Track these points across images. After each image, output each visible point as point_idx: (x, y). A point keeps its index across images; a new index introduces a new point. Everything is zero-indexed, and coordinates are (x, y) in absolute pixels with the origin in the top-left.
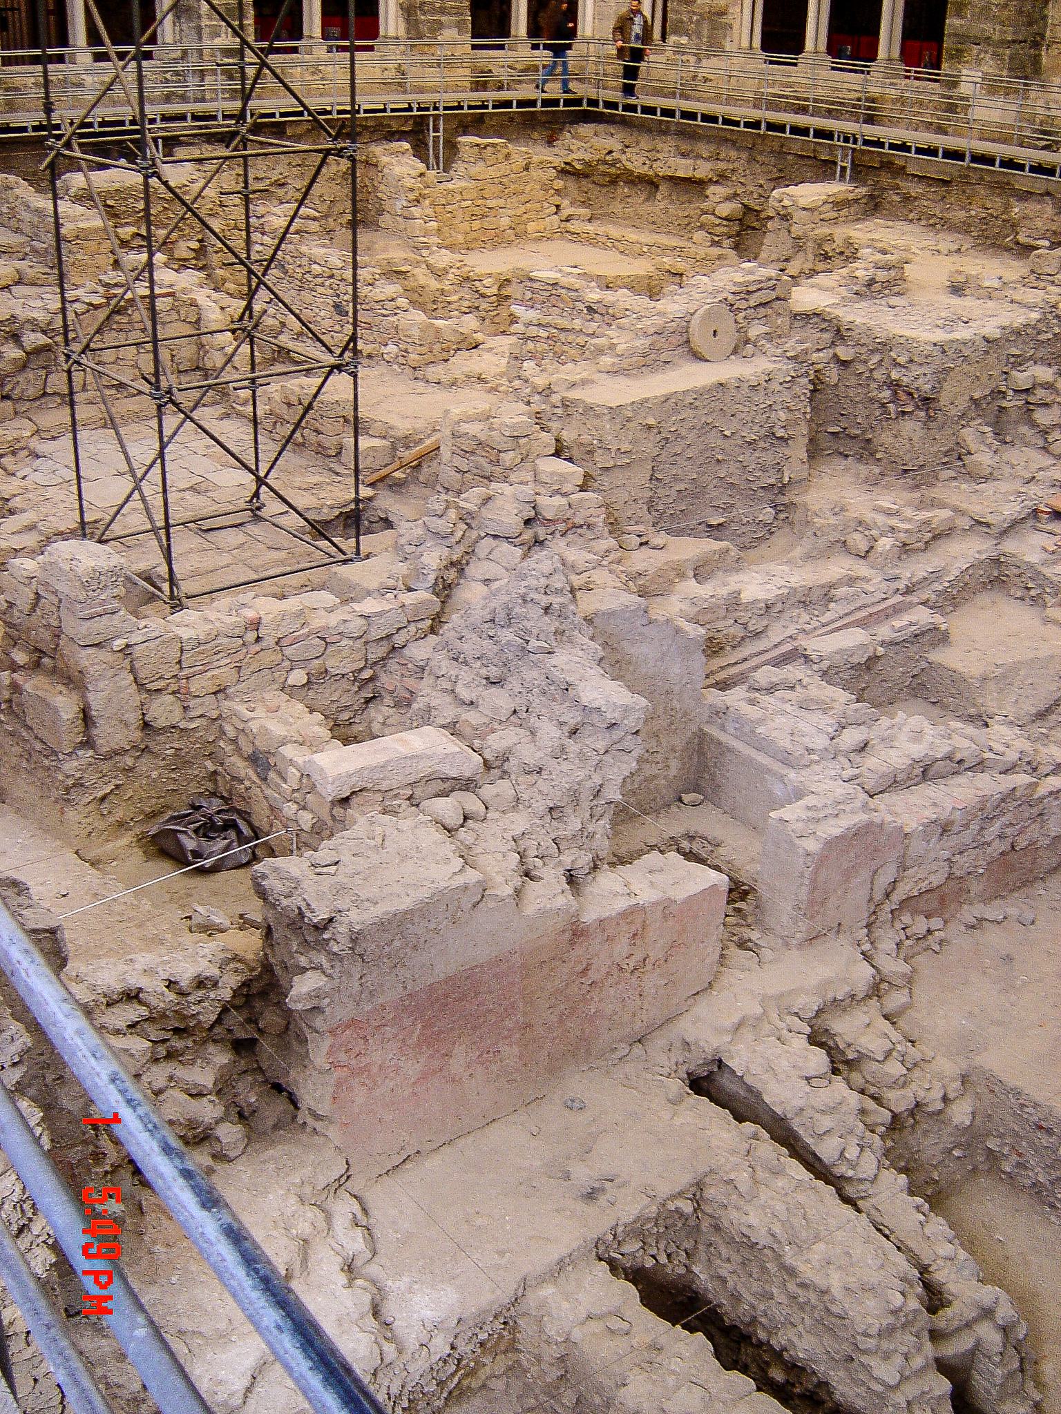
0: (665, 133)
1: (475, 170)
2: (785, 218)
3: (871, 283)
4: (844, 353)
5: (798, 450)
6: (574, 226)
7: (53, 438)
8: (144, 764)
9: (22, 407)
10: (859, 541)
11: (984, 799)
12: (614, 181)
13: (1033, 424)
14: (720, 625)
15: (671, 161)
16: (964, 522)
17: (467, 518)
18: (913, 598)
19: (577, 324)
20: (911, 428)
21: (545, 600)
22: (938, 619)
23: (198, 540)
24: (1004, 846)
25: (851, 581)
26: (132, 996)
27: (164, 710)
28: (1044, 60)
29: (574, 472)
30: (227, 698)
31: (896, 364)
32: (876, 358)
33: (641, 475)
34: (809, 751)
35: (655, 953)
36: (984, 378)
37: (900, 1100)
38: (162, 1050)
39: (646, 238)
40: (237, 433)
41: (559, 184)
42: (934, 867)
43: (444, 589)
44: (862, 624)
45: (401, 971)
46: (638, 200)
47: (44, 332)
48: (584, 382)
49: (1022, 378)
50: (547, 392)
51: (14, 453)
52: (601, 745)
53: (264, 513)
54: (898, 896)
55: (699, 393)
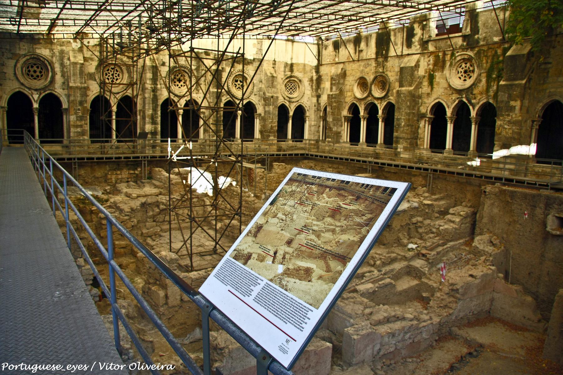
0: (325, 162)
1: (278, 170)
7: (166, 232)
9: (158, 224)
11: (404, 328)
13: (417, 232)
16: (399, 257)
22: (392, 281)
24: (411, 341)
25: (370, 272)
28: (419, 143)
34: (356, 314)
35: (312, 364)
36: (404, 220)
40: (212, 233)
44: (372, 283)
45: (242, 363)
47: (165, 205)
49: (414, 220)
51: (155, 235)
54: (381, 353)
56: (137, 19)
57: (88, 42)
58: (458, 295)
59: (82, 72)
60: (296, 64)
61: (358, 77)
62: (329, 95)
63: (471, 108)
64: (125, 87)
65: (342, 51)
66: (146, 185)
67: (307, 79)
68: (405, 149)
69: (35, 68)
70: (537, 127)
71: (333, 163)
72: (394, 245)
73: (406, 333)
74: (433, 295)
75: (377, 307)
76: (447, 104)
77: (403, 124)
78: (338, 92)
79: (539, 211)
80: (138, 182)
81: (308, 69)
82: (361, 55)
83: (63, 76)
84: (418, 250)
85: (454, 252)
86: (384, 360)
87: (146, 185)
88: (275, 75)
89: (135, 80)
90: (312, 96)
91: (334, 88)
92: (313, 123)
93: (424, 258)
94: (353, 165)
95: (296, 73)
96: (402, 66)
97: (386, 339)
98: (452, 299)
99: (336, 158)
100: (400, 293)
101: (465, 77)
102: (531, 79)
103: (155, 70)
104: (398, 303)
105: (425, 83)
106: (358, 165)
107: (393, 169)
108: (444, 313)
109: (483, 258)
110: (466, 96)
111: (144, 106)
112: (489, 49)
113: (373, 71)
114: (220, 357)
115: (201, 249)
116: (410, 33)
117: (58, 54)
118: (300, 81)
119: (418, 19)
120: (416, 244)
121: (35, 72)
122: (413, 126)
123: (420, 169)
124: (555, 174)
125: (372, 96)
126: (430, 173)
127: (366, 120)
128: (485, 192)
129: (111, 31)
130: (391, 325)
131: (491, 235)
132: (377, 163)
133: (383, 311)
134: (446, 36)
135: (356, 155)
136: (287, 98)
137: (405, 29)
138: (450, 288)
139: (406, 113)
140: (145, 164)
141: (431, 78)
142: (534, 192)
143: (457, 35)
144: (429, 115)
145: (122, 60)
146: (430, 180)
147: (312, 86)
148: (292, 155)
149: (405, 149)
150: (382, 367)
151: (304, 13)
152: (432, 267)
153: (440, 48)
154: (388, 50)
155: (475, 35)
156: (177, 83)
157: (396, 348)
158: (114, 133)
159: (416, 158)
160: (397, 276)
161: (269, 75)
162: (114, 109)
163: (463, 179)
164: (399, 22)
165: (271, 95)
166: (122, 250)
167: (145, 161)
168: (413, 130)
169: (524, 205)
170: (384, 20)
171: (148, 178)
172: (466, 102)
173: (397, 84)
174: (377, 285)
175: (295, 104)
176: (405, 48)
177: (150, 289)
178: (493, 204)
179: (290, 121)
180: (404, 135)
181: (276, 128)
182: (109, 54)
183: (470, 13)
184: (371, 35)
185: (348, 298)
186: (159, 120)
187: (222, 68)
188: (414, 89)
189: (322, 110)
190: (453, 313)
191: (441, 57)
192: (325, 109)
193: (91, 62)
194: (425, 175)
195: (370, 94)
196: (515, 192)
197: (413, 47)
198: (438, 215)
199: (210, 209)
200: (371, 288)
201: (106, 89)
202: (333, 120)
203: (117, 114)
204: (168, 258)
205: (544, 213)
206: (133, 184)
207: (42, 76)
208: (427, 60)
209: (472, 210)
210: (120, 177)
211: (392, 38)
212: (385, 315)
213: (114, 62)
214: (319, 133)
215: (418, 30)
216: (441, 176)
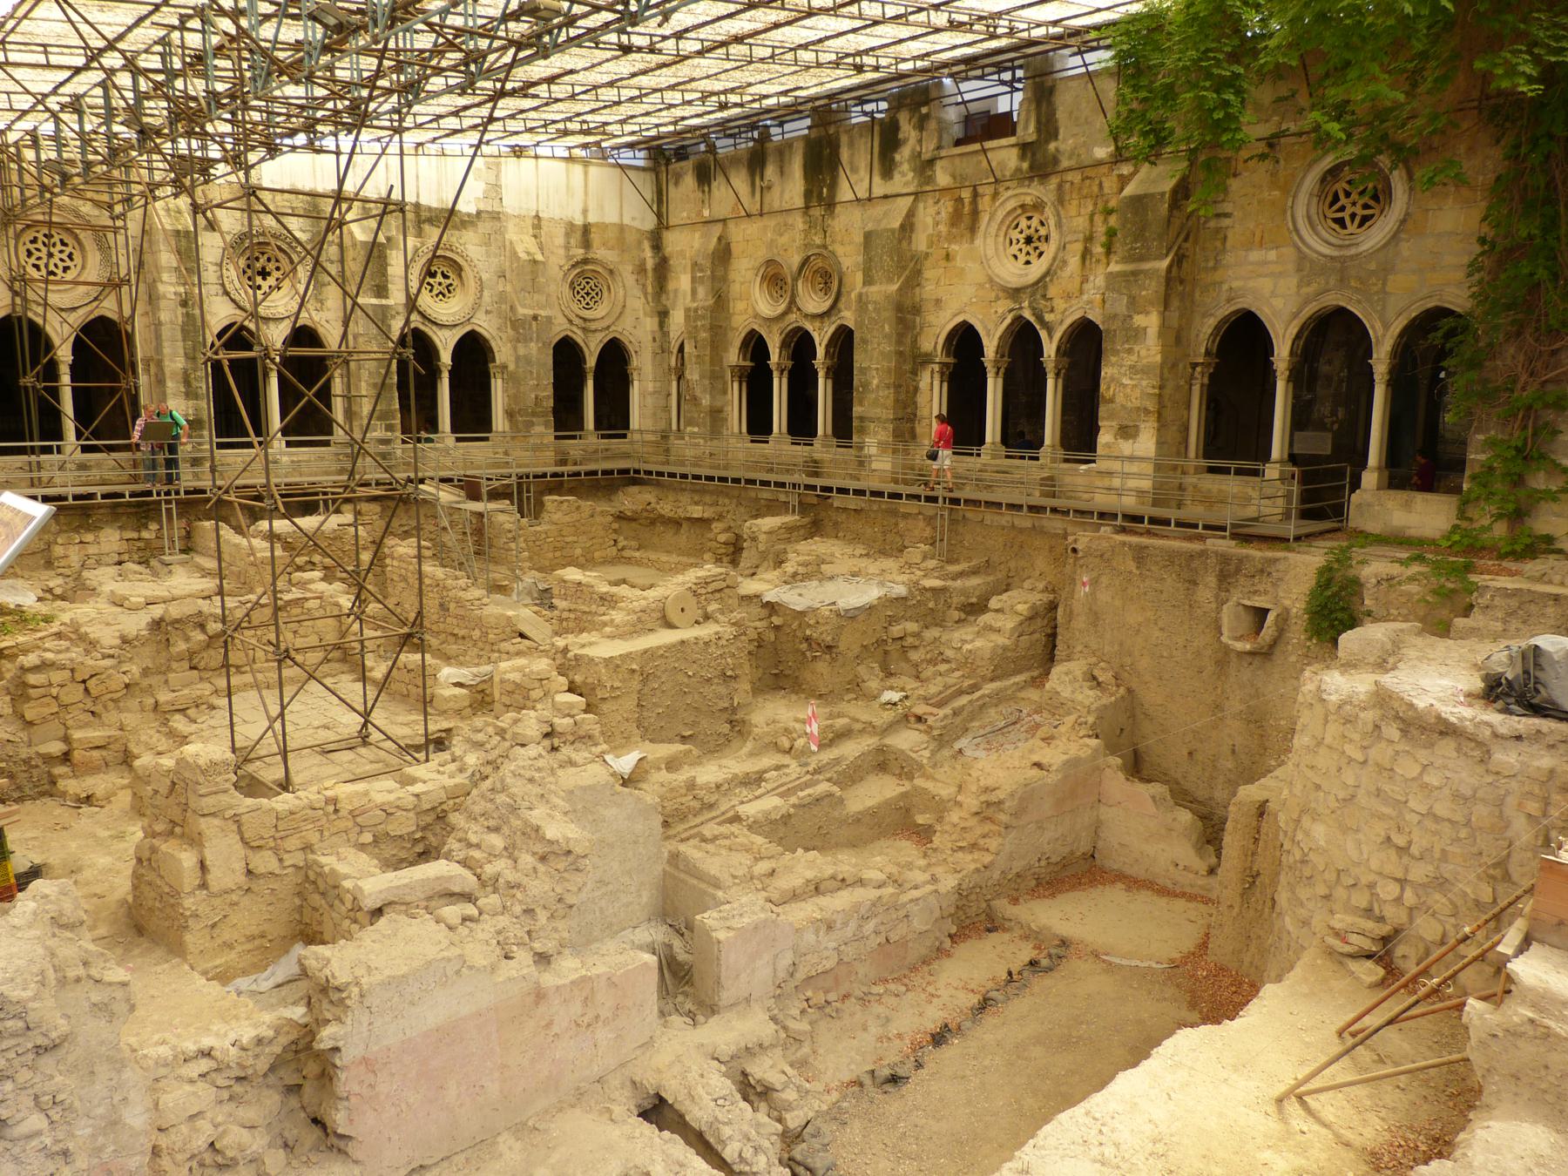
1: (555, 517)
2: (754, 539)
3: (795, 575)
4: (776, 620)
5: (744, 686)
6: (627, 553)
8: (246, 901)
9: (206, 675)
10: (786, 744)
11: (856, 907)
12: (653, 522)
13: (907, 660)
14: (684, 800)
15: (689, 508)
17: (501, 733)
20: (822, 667)
21: (528, 774)
22: (835, 789)
23: (319, 757)
25: (778, 768)
26: (207, 1054)
27: (265, 862)
28: (918, 430)
30: (313, 852)
31: (809, 626)
32: (795, 626)
33: (630, 703)
34: (735, 877)
35: (605, 1013)
37: (794, 1120)
38: (225, 1095)
39: (674, 558)
41: (615, 526)
42: (826, 953)
44: (781, 795)
46: (669, 536)
48: (591, 644)
49: (896, 630)
50: (566, 650)
52: (561, 866)
53: (371, 739)
54: (800, 976)
55: (669, 648)
58: (1003, 817)
60: (597, 225)
61: (761, 260)
63: (1043, 334)
64: (94, 291)
65: (719, 189)
66: (178, 569)
67: (630, 268)
70: (1206, 381)
71: (703, 492)
73: (865, 919)
74: (940, 819)
75: (788, 856)
76: (985, 327)
77: (875, 382)
78: (711, 302)
79: (1206, 593)
80: (153, 562)
81: (631, 238)
85: (1000, 708)
86: (809, 994)
87: (178, 569)
88: (539, 257)
89: (123, 272)
92: (650, 387)
94: (753, 494)
95: (599, 253)
96: (870, 227)
97: (810, 937)
98: (988, 827)
100: (857, 820)
102: (1184, 256)
103: (184, 242)
104: (853, 844)
109: (1070, 719)
111: (159, 348)
113: (798, 243)
114: (338, 1011)
118: (611, 272)
120: (903, 690)
124: (1251, 498)
128: (1074, 550)
129: (26, 124)
130: (823, 901)
131: (1094, 660)
132: (814, 488)
133: (805, 865)
134: (977, 146)
136: (577, 321)
137: (877, 128)
138: (983, 798)
139: (882, 353)
140: (169, 511)
142: (1196, 546)
143: (1004, 142)
144: (940, 357)
145: (77, 214)
147: (644, 286)
148: (594, 473)
150: (803, 1012)
152: (941, 747)
153: (964, 178)
154: (833, 186)
155: (1047, 142)
156: (259, 280)
158: (69, 427)
160: (851, 776)
162: (64, 354)
163: (1024, 520)
165: (531, 312)
166: (96, 753)
167: (168, 502)
168: (902, 397)
171: (182, 551)
172: (1032, 319)
173: (859, 277)
174: (793, 800)
175: (599, 336)
176: (877, 179)
177: (154, 850)
179: (590, 384)
180: (877, 412)
181: (551, 403)
182: (28, 193)
185: (716, 838)
187: (389, 239)
188: (900, 289)
189: (675, 351)
190: (992, 863)
191: (967, 201)
192: (681, 349)
194: (931, 513)
197: (897, 176)
198: (963, 616)
200: (775, 808)
201: (31, 295)
202: (702, 377)
203: (73, 368)
204: (201, 762)
205: (1217, 597)
208: (932, 210)
210: (92, 550)
211: (845, 154)
212: (810, 874)
214: (669, 412)
216: (969, 515)
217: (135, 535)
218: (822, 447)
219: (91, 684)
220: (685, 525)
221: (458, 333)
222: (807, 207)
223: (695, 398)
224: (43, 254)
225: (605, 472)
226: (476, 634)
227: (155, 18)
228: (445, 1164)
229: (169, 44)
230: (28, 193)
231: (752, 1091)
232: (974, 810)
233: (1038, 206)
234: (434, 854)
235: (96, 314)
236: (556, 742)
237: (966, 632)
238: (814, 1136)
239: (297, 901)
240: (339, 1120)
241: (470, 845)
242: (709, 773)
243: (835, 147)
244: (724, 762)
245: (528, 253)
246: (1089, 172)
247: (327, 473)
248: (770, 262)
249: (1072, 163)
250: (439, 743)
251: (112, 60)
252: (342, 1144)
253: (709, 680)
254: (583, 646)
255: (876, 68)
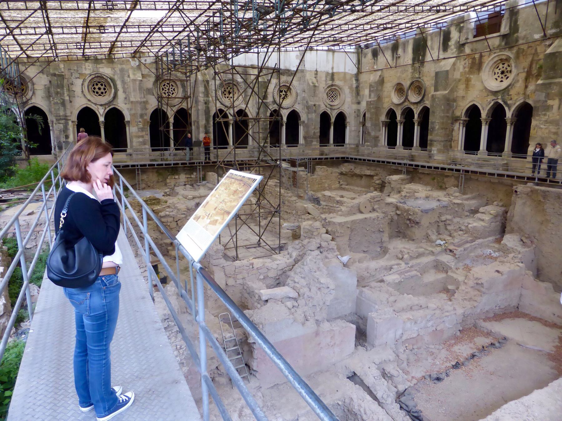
0: (363, 165)
1: (320, 173)
2: (390, 183)
3: (405, 196)
4: (398, 212)
6: (343, 186)
13: (446, 229)
14: (364, 273)
18: (413, 269)
19: (335, 205)
22: (418, 274)
25: (398, 264)
28: (453, 145)
29: (330, 237)
31: (410, 215)
32: (405, 214)
33: (347, 238)
37: (401, 388)
39: (359, 189)
40: (257, 229)
41: (339, 177)
43: (296, 261)
44: (399, 274)
48: (334, 217)
49: (443, 218)
50: (325, 219)
53: (261, 245)
54: (404, 338)
55: (361, 220)
56: (187, 38)
57: (146, 60)
58: (482, 289)
59: (141, 88)
62: (367, 102)
63: (506, 109)
64: (180, 100)
65: (381, 58)
68: (439, 151)
69: (99, 86)
71: (370, 165)
72: (423, 241)
74: (458, 288)
75: (401, 296)
76: (482, 106)
77: (437, 127)
78: (376, 99)
80: (194, 185)
81: (348, 77)
82: (399, 61)
83: (124, 92)
84: (445, 246)
86: (407, 345)
87: (202, 188)
88: (317, 85)
89: (189, 94)
90: (352, 103)
91: (373, 95)
92: (353, 129)
93: (451, 254)
94: (389, 167)
95: (337, 82)
98: (477, 293)
99: (374, 161)
100: (426, 285)
101: (502, 78)
105: (462, 86)
106: (394, 168)
107: (426, 171)
108: (468, 305)
109: (511, 255)
110: (502, 97)
112: (529, 47)
115: (247, 243)
116: (446, 37)
117: (119, 72)
118: (340, 89)
119: (455, 22)
120: (445, 240)
121: (99, 89)
122: (447, 129)
123: (452, 170)
125: (409, 101)
126: (462, 174)
127: (402, 124)
128: (516, 191)
130: (413, 313)
132: (412, 165)
133: (408, 299)
134: (483, 37)
135: (392, 158)
136: (328, 106)
137: (442, 33)
138: (475, 282)
140: (199, 169)
141: (468, 81)
144: (463, 118)
145: (176, 76)
146: (462, 181)
148: (333, 158)
149: (439, 151)
150: (404, 351)
151: (340, 25)
153: (476, 50)
154: (424, 55)
157: (418, 335)
158: (172, 143)
159: (450, 159)
160: (424, 271)
161: (311, 84)
162: (171, 120)
163: (495, 179)
164: (435, 26)
165: (313, 103)
167: (199, 166)
168: (448, 132)
169: (557, 205)
170: (420, 25)
172: (502, 103)
173: (433, 88)
174: (403, 276)
175: (336, 111)
176: (441, 52)
178: (524, 204)
179: (332, 128)
181: (319, 134)
182: (164, 71)
183: (510, 11)
184: (408, 41)
185: (375, 287)
186: (211, 129)
189: (362, 116)
192: (364, 115)
193: (149, 79)
194: (456, 175)
195: (406, 99)
196: (548, 191)
197: (449, 50)
198: (468, 214)
199: (255, 206)
201: (163, 102)
202: (372, 125)
206: (190, 186)
207: (106, 92)
208: (463, 63)
209: (503, 209)
211: (429, 43)
213: (169, 78)
215: (455, 35)
216: (472, 177)
217: (189, 176)
218: (416, 149)
219: (179, 222)
220: (364, 177)
221: (289, 111)
222: (413, 64)
223: (369, 133)
224: (170, 90)
225: (337, 158)
226: (294, 212)
227: (205, 14)
228: (284, 385)
229: (209, 22)
230: (164, 71)
231: (384, 375)
232: (472, 286)
233: (508, 59)
234: (282, 284)
235: (181, 107)
236: (322, 250)
237: (470, 220)
238: (408, 395)
239: (240, 295)
240: (254, 365)
241: (295, 282)
242: (373, 265)
243: (425, 40)
244: (378, 261)
245: (313, 83)
246: (530, 44)
247: (246, 157)
248: (399, 84)
249: (524, 41)
250: (281, 248)
251: (192, 28)
252: (254, 373)
253: (374, 232)
254: (331, 218)
255: (445, 11)
